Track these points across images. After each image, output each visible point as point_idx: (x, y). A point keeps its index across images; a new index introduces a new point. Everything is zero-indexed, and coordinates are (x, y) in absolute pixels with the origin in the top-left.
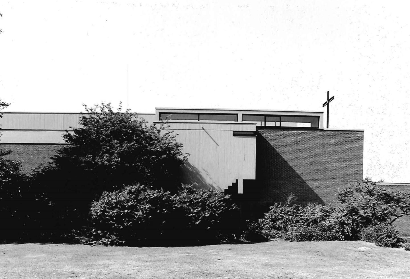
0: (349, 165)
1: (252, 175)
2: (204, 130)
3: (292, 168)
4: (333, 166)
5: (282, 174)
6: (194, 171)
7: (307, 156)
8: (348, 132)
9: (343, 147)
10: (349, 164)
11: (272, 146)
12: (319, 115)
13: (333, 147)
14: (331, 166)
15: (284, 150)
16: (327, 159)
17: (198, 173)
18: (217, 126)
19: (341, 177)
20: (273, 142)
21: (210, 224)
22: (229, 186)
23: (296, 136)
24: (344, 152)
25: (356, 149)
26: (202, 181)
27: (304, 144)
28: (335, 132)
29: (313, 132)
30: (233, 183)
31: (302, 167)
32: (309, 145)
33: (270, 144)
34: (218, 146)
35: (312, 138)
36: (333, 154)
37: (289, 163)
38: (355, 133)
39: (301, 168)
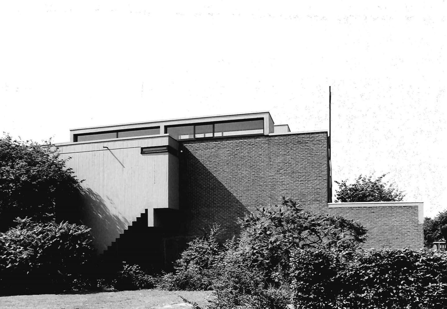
0: (307, 181)
1: (164, 203)
2: (109, 150)
3: (228, 191)
4: (283, 184)
5: (215, 199)
6: (98, 201)
7: (247, 173)
8: (303, 136)
9: (297, 156)
10: (306, 180)
11: (202, 163)
12: (263, 117)
13: (283, 158)
14: (281, 184)
15: (217, 168)
16: (275, 175)
17: (101, 203)
18: (123, 144)
19: (295, 199)
20: (202, 158)
21: (28, 268)
22: (137, 218)
23: (232, 147)
24: (299, 164)
25: (316, 159)
26: (106, 212)
27: (242, 157)
28: (285, 137)
29: (255, 140)
30: (142, 214)
31: (241, 189)
32: (249, 159)
33: (199, 161)
34: (124, 168)
35: (254, 148)
36: (283, 168)
37: (223, 184)
38: (314, 136)
39: (239, 189)
